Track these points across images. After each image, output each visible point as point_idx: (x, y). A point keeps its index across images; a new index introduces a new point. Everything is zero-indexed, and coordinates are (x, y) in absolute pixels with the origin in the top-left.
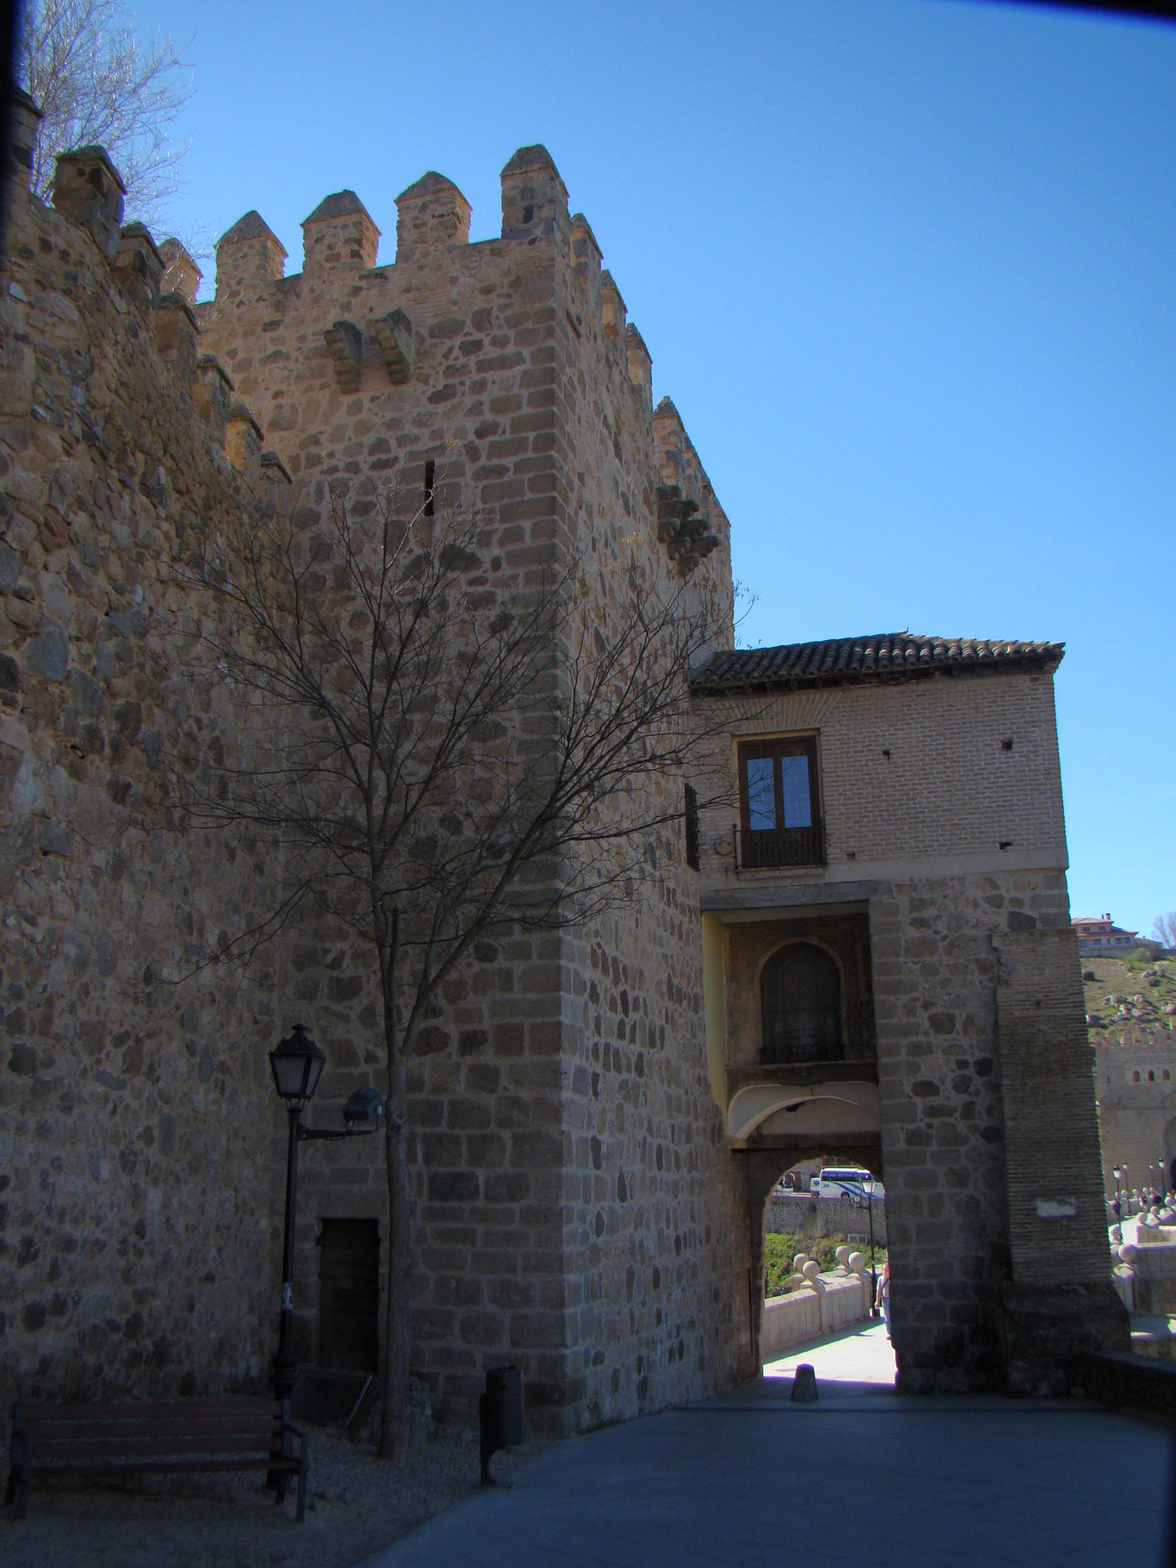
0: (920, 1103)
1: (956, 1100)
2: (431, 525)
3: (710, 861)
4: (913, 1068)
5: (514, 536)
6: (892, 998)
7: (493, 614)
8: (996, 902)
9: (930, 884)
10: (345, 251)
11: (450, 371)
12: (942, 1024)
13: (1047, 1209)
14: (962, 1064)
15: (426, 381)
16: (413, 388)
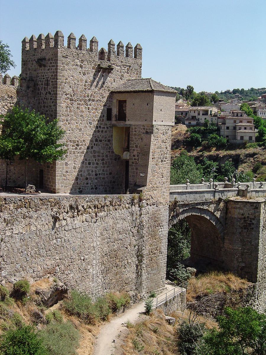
0: (134, 158)
1: (137, 158)
2: (47, 88)
3: (114, 119)
4: (133, 153)
5: (54, 91)
6: (131, 142)
7: (52, 100)
8: (144, 129)
9: (137, 125)
10: (40, 45)
11: (50, 66)
12: (136, 146)
13: (141, 175)
14: (138, 153)
15: (47, 67)
16: (46, 68)
